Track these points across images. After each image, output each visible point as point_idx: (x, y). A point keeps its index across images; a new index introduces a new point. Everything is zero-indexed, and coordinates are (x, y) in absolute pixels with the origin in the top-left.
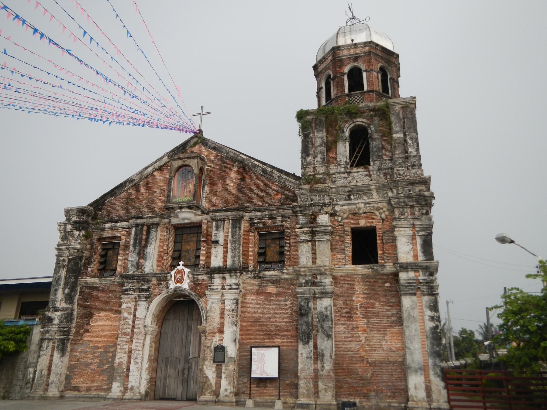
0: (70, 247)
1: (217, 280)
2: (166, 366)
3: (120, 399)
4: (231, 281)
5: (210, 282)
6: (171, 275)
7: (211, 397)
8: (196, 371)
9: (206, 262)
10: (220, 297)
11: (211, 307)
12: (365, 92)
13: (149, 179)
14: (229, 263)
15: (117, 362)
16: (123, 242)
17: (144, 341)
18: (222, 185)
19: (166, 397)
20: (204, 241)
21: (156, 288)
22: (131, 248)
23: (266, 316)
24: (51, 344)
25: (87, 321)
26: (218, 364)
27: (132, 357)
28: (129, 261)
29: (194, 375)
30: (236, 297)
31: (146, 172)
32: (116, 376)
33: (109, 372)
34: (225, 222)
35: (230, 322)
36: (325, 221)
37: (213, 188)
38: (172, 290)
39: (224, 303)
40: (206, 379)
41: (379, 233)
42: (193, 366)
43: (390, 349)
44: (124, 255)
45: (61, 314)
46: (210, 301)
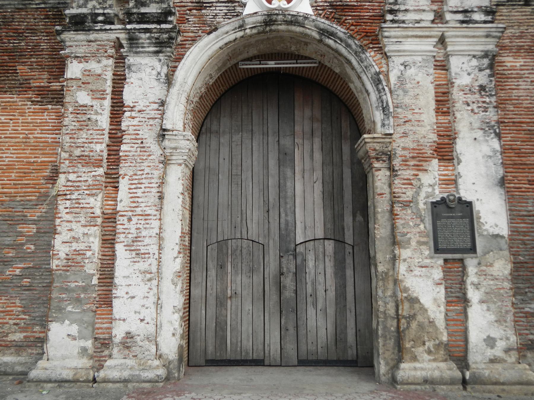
2: (222, 267)
3: (87, 381)
7: (443, 365)
8: (321, 279)
10: (431, 48)
11: (401, 79)
15: (62, 255)
17: (162, 183)
19: (229, 355)
21: (192, 19)
26: (449, 256)
27: (121, 237)
29: (315, 290)
30: (491, 47)
32: (62, 300)
33: (29, 288)
35: (477, 125)
38: (260, 18)
40: (412, 307)
42: (311, 264)
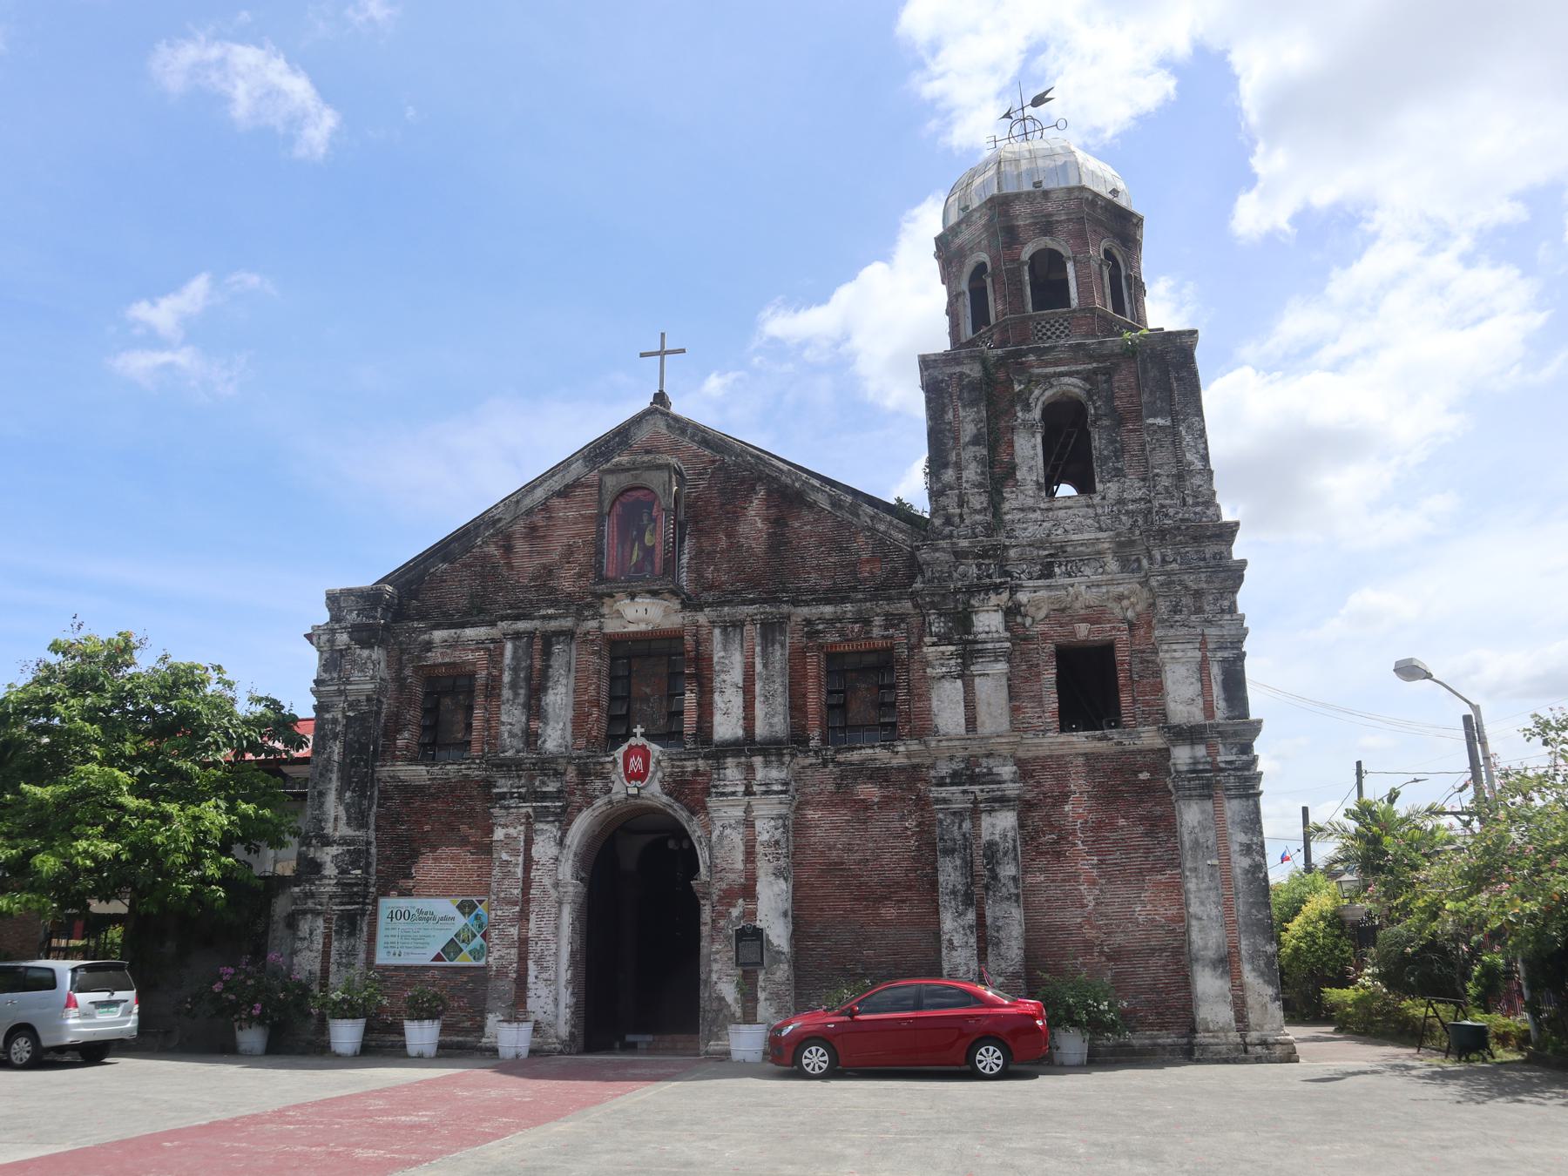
0: (348, 687)
1: (732, 773)
4: (764, 772)
5: (716, 776)
6: (614, 759)
9: (699, 729)
12: (1074, 311)
13: (538, 519)
14: (760, 730)
16: (482, 675)
18: (729, 536)
20: (690, 676)
22: (507, 693)
23: (857, 856)
24: (320, 922)
25: (403, 868)
27: (531, 955)
28: (503, 724)
30: (784, 811)
31: (528, 502)
34: (745, 628)
36: (994, 629)
37: (706, 544)
39: (753, 826)
41: (1121, 655)
43: (1153, 920)
44: (486, 709)
45: (340, 851)
46: (719, 824)
